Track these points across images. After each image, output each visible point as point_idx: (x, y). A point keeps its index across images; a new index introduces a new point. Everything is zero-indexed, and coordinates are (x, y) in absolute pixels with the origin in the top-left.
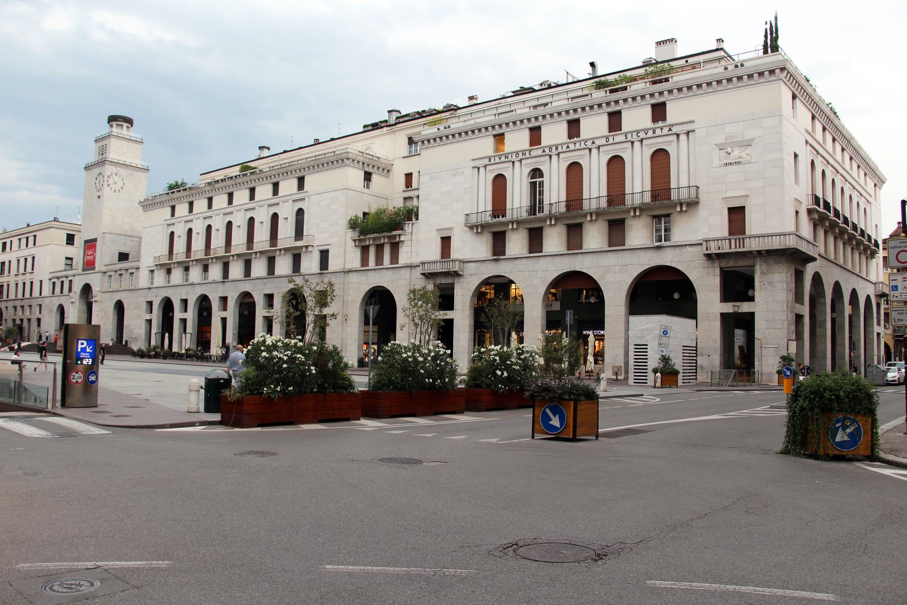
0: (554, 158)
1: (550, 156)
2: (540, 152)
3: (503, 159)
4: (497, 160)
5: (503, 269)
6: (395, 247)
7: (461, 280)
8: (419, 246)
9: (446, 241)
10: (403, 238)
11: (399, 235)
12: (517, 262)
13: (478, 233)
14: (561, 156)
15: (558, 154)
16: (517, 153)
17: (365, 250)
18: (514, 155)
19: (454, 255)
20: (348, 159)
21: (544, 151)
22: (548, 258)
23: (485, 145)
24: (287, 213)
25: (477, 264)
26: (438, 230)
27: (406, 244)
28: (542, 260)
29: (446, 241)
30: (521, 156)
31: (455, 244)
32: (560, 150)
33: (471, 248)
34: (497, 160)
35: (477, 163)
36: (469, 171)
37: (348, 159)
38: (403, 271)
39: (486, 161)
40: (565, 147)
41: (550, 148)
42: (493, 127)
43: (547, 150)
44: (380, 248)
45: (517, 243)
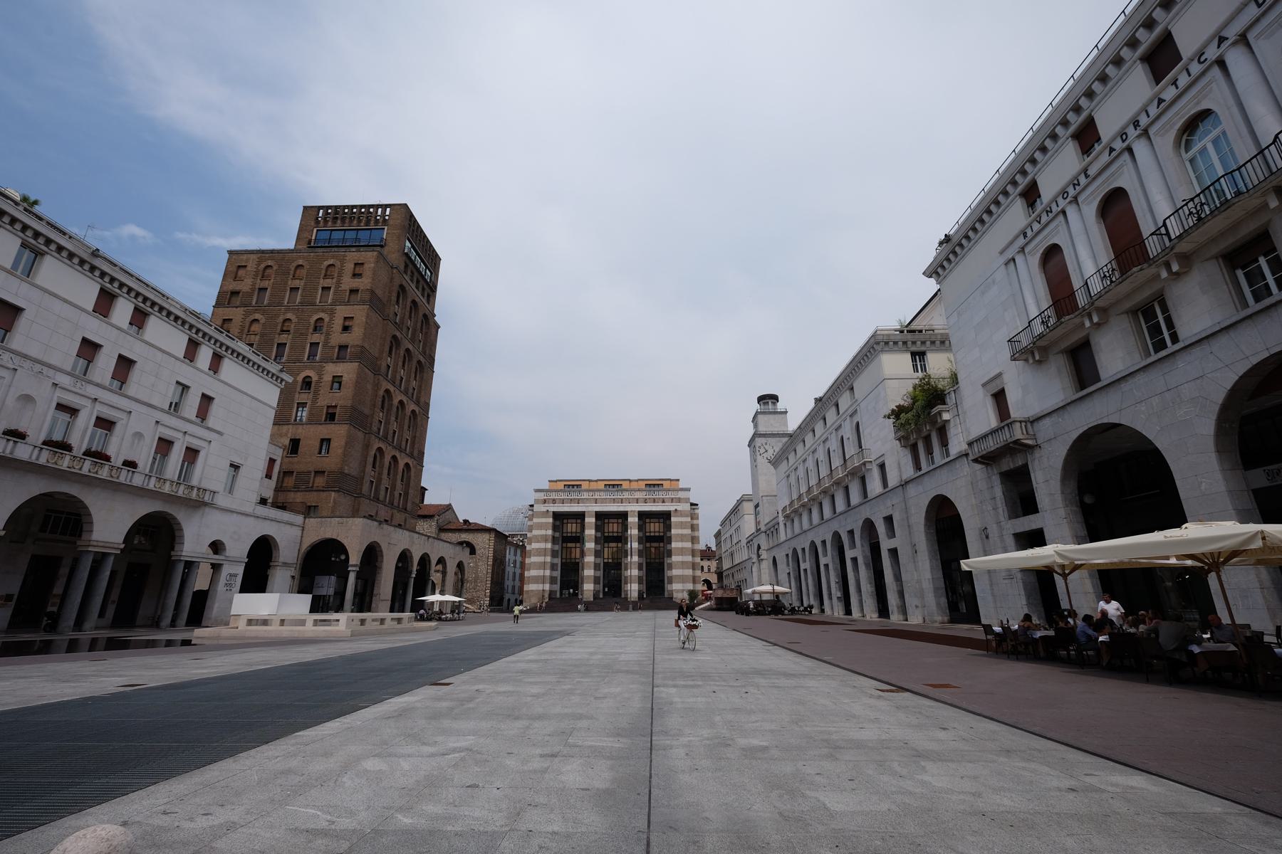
0: (1140, 149)
1: (1130, 150)
2: (1105, 158)
3: (1044, 219)
4: (1036, 227)
5: (1099, 411)
6: (942, 431)
7: (1037, 454)
8: (971, 420)
9: (999, 397)
10: (946, 416)
11: (940, 413)
12: (1125, 387)
13: (1040, 362)
14: (1151, 132)
15: (1145, 133)
16: (1064, 193)
17: (914, 449)
18: (1060, 200)
19: (1015, 413)
20: (878, 343)
21: (1112, 150)
22: (1197, 351)
23: (1015, 215)
24: (848, 431)
25: (1054, 418)
26: (984, 385)
27: (952, 424)
28: (1181, 363)
29: (999, 397)
30: (1072, 192)
31: (1012, 398)
32: (1144, 121)
33: (1035, 392)
34: (1036, 227)
35: (1009, 255)
36: (1001, 274)
37: (878, 343)
38: (958, 464)
39: (1021, 241)
40: (1153, 111)
41: (1123, 135)
42: (1014, 183)
43: (1118, 145)
44: (927, 440)
45: (1115, 352)
